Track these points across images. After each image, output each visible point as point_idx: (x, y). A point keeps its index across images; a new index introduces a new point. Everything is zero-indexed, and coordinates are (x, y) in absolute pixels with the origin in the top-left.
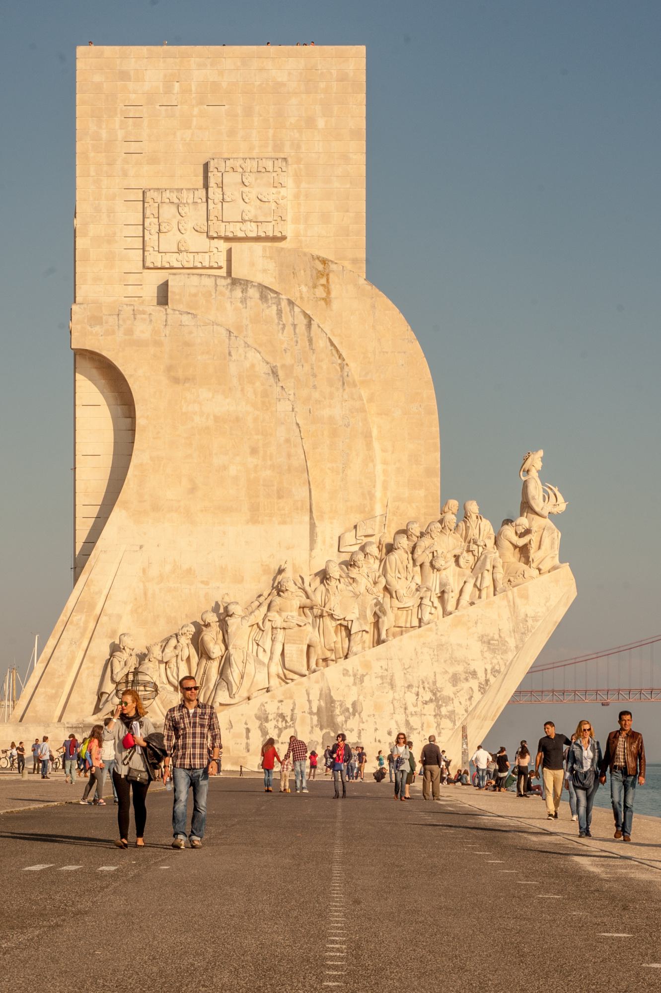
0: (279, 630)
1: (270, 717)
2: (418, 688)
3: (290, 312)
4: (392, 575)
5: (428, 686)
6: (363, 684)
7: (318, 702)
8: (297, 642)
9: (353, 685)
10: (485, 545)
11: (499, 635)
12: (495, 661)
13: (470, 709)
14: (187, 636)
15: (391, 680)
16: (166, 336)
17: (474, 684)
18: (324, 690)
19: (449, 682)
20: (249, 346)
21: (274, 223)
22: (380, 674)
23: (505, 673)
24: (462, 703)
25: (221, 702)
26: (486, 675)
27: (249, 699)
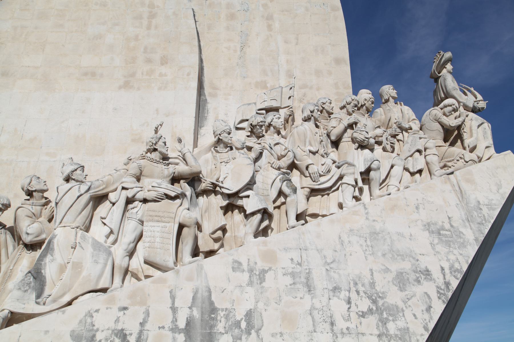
2: (349, 291)
4: (302, 148)
5: (363, 289)
6: (264, 284)
8: (166, 219)
9: (248, 285)
10: (411, 129)
11: (450, 224)
12: (452, 257)
13: (431, 326)
15: (307, 279)
17: (430, 288)
18: (200, 291)
22: (290, 270)
23: (465, 277)
24: (417, 316)
26: (444, 275)
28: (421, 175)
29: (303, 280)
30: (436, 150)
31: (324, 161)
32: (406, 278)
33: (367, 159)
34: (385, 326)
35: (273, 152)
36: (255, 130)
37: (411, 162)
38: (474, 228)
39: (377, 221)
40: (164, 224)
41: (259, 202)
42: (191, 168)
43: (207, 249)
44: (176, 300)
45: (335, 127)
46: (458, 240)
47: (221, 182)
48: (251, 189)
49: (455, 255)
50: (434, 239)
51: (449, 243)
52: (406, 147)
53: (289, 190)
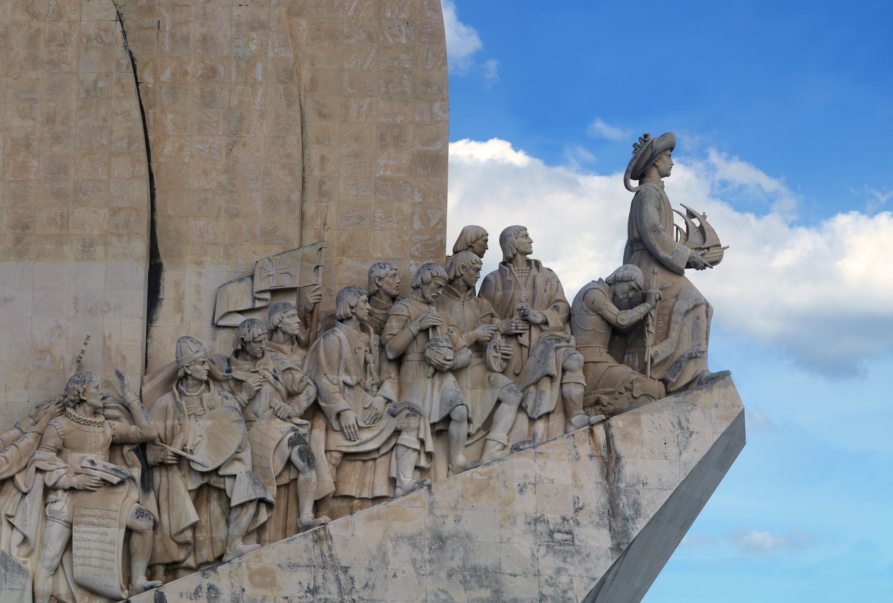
0: (60, 492)
8: (106, 521)
10: (546, 323)
30: (583, 375)
31: (370, 403)
33: (446, 399)
35: (280, 386)
37: (533, 396)
40: (101, 529)
41: (251, 488)
43: (167, 560)
45: (395, 335)
46: (581, 550)
47: (189, 452)
48: (239, 460)
50: (541, 547)
52: (531, 362)
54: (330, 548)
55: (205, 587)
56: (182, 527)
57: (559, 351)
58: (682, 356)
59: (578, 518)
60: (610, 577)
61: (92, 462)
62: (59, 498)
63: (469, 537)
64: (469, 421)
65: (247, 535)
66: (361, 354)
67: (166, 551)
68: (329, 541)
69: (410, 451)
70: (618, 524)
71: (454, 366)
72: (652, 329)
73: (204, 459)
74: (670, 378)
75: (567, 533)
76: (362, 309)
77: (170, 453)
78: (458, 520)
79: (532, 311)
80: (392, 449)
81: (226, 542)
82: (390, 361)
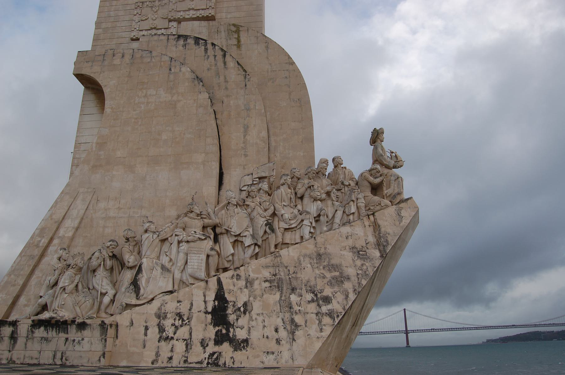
0: (184, 243)
1: (169, 316)
2: (301, 290)
3: (213, 49)
5: (310, 288)
7: (213, 301)
8: (200, 252)
10: (350, 185)
13: (347, 307)
14: (110, 249)
16: (131, 63)
17: (348, 286)
19: (328, 284)
20: (183, 65)
21: (207, 10)
22: (269, 279)
23: (373, 278)
25: (128, 303)
26: (359, 278)
27: (153, 299)
28: (353, 215)
29: (276, 284)
30: (363, 200)
32: (335, 281)
34: (320, 308)
35: (262, 207)
36: (250, 194)
38: (381, 249)
39: (321, 248)
40: (198, 255)
42: (213, 221)
43: (223, 267)
44: (206, 297)
45: (300, 189)
49: (367, 266)
51: (364, 259)
52: (347, 197)
53: (270, 231)
54: (280, 260)
55: (235, 275)
56: (228, 255)
57: (355, 193)
58: (396, 194)
59: (367, 246)
60: (381, 267)
61: (195, 232)
62: (183, 245)
63: (330, 254)
64: (327, 217)
65: (251, 257)
66: (289, 196)
67: (223, 264)
68: (280, 257)
69: (307, 226)
70: (381, 248)
71: (320, 199)
72: (385, 185)
73: (235, 230)
74: (392, 200)
75: (364, 251)
76: (288, 181)
77: (223, 229)
78: (325, 248)
79: (345, 181)
80: (301, 227)
81: (243, 260)
82: (299, 198)
